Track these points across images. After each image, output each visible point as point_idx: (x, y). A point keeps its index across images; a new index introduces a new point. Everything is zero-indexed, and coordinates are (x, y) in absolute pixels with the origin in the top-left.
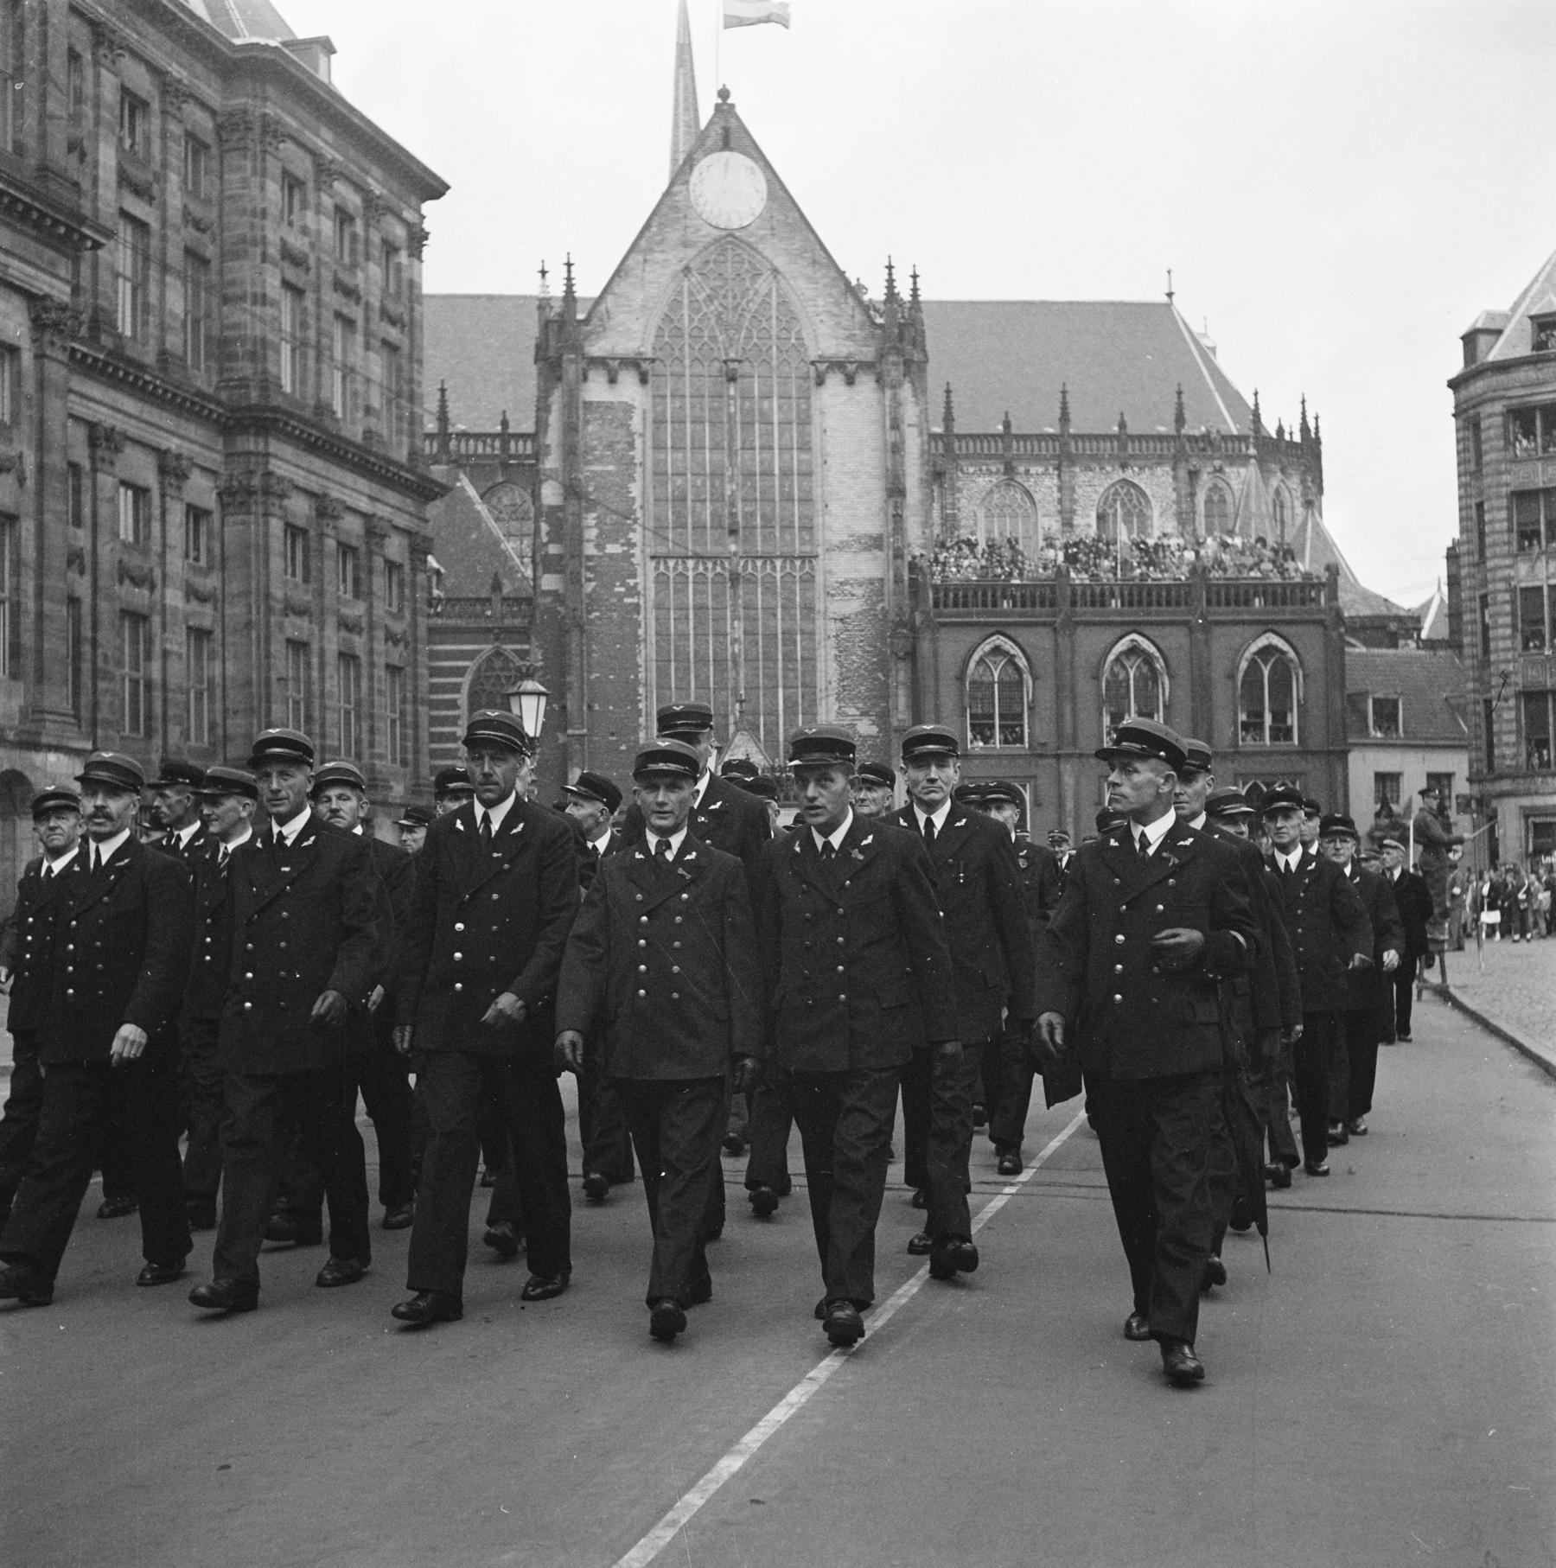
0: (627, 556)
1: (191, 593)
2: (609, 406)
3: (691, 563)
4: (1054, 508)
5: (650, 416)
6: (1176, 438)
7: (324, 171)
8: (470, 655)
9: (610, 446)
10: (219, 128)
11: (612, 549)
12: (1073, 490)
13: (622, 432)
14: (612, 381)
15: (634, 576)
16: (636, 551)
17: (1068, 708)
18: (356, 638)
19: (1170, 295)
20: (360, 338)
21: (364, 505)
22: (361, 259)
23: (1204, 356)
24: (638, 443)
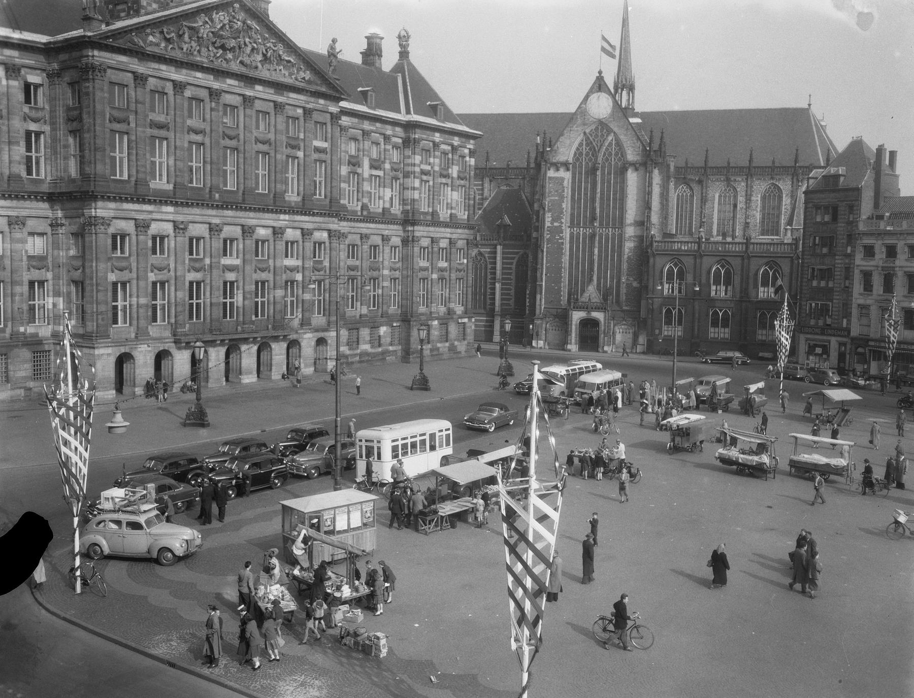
1: (392, 269)
2: (556, 178)
3: (581, 229)
4: (744, 193)
5: (570, 181)
6: (795, 167)
7: (436, 145)
8: (517, 253)
9: (557, 191)
10: (404, 142)
11: (556, 224)
12: (752, 187)
14: (558, 170)
16: (563, 225)
18: (445, 273)
19: (809, 105)
20: (450, 189)
21: (448, 236)
22: (450, 165)
23: (818, 131)
24: (566, 191)
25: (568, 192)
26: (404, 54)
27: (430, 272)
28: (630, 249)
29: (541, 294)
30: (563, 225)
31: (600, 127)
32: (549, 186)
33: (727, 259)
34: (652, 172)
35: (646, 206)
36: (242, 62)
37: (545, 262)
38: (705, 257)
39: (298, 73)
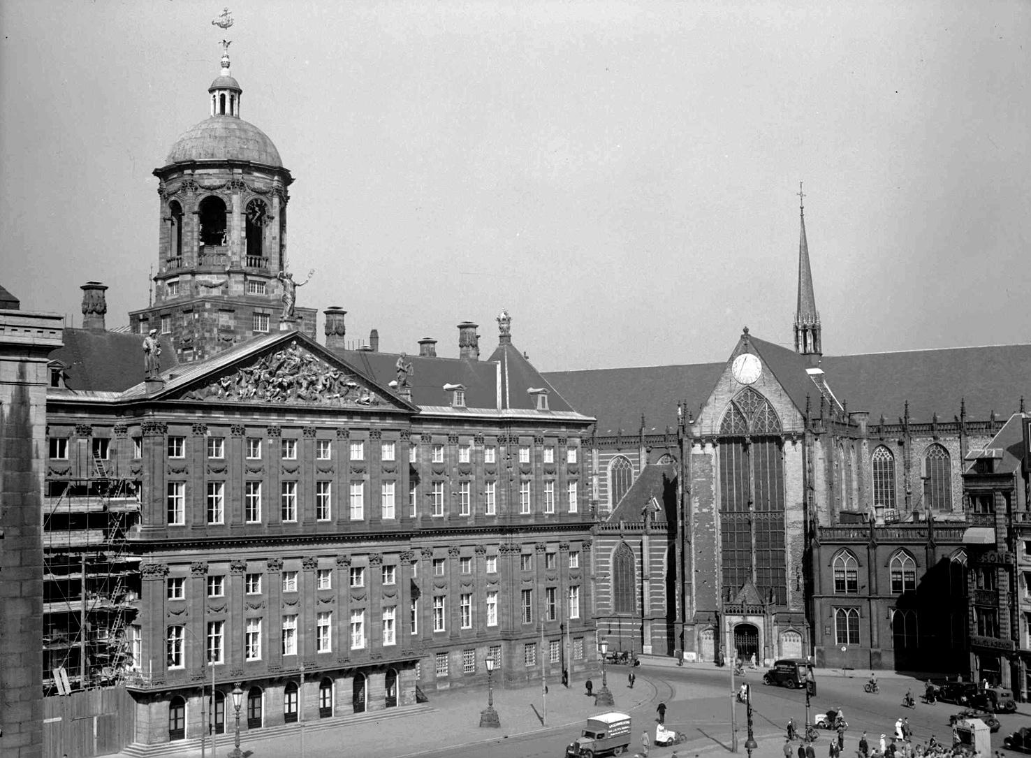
0: (710, 513)
11: (705, 510)
13: (707, 465)
14: (703, 447)
15: (713, 521)
17: (874, 579)
21: (557, 539)
25: (716, 472)
26: (505, 337)
27: (535, 582)
28: (794, 538)
29: (691, 594)
30: (713, 511)
31: (749, 394)
32: (694, 467)
33: (908, 547)
34: (812, 444)
35: (808, 487)
36: (299, 396)
37: (693, 556)
38: (880, 547)
39: (361, 396)
